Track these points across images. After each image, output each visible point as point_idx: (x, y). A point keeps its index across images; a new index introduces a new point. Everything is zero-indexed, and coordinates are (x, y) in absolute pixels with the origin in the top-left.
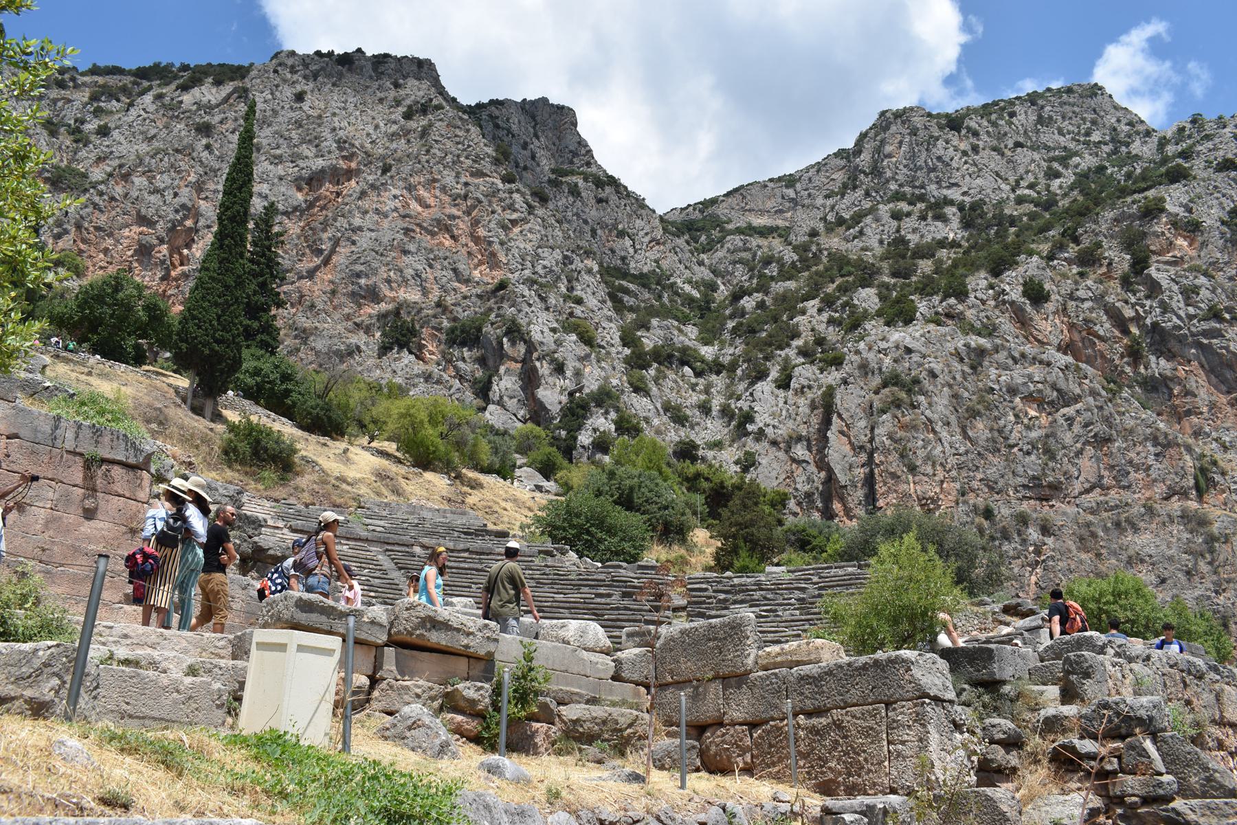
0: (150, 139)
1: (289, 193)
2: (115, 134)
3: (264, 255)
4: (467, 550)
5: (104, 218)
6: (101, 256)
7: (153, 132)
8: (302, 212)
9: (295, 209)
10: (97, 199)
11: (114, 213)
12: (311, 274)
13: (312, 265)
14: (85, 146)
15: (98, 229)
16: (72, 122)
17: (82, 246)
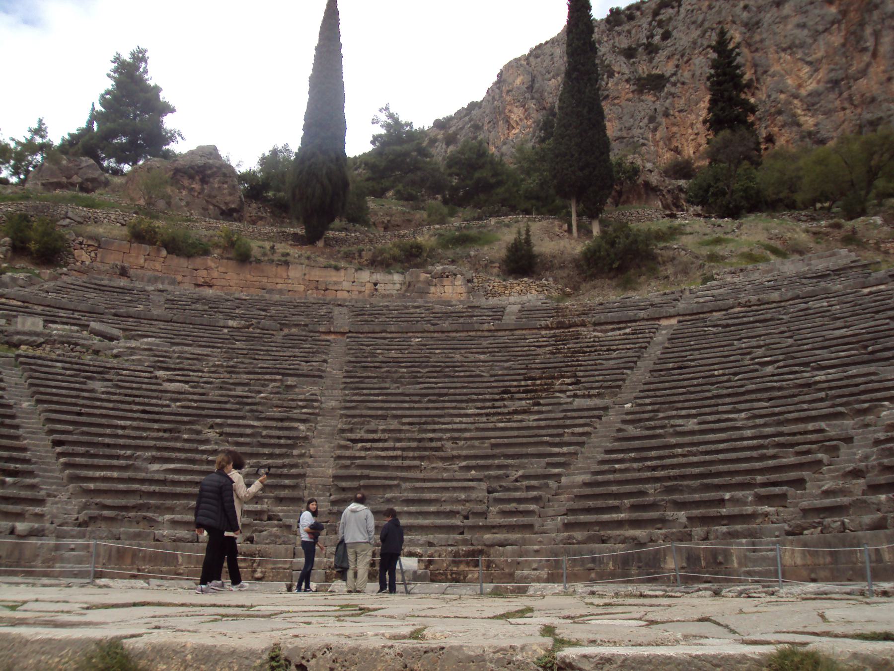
0: (701, 25)
1: (823, 12)
2: (675, 33)
3: (725, 74)
4: (798, 297)
5: (682, 101)
6: (690, 131)
7: (701, 18)
8: (839, 22)
9: (833, 23)
10: (673, 90)
11: (688, 94)
12: (864, 73)
13: (862, 65)
14: (657, 53)
15: (680, 111)
16: (645, 41)
17: (675, 129)
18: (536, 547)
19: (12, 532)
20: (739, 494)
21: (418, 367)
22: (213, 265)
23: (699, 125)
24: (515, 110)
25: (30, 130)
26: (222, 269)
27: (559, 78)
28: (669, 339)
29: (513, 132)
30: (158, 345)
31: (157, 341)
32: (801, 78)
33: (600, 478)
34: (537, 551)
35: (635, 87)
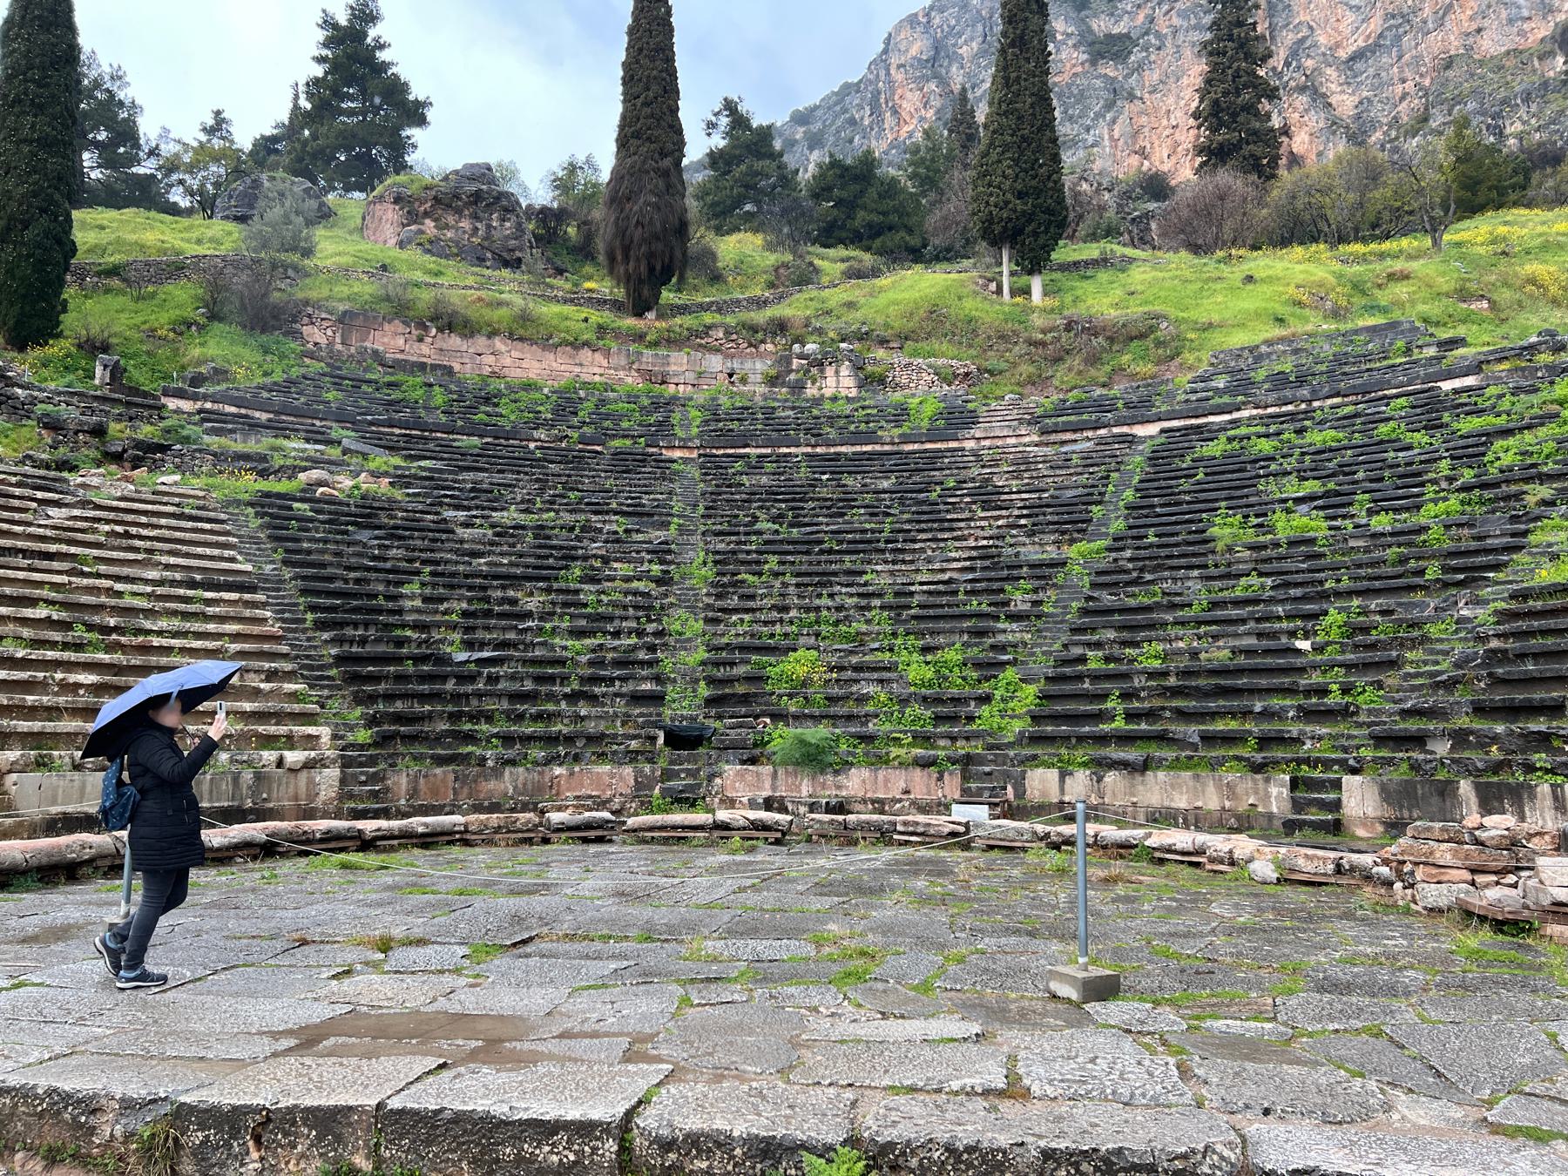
3: (1231, 38)
6: (1165, 122)
17: (1144, 119)
18: (987, 769)
19: (280, 763)
20: (1276, 702)
21: (801, 500)
22: (503, 348)
23: (1179, 114)
24: (909, 95)
25: (204, 129)
26: (515, 354)
27: (974, 44)
28: (1150, 459)
29: (906, 128)
30: (440, 471)
31: (439, 465)
32: (1340, 33)
33: (1067, 670)
34: (989, 774)
35: (1086, 56)
